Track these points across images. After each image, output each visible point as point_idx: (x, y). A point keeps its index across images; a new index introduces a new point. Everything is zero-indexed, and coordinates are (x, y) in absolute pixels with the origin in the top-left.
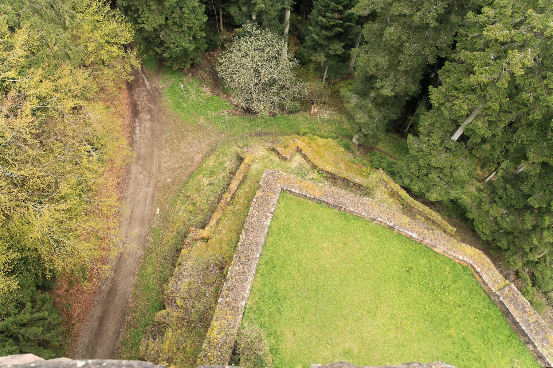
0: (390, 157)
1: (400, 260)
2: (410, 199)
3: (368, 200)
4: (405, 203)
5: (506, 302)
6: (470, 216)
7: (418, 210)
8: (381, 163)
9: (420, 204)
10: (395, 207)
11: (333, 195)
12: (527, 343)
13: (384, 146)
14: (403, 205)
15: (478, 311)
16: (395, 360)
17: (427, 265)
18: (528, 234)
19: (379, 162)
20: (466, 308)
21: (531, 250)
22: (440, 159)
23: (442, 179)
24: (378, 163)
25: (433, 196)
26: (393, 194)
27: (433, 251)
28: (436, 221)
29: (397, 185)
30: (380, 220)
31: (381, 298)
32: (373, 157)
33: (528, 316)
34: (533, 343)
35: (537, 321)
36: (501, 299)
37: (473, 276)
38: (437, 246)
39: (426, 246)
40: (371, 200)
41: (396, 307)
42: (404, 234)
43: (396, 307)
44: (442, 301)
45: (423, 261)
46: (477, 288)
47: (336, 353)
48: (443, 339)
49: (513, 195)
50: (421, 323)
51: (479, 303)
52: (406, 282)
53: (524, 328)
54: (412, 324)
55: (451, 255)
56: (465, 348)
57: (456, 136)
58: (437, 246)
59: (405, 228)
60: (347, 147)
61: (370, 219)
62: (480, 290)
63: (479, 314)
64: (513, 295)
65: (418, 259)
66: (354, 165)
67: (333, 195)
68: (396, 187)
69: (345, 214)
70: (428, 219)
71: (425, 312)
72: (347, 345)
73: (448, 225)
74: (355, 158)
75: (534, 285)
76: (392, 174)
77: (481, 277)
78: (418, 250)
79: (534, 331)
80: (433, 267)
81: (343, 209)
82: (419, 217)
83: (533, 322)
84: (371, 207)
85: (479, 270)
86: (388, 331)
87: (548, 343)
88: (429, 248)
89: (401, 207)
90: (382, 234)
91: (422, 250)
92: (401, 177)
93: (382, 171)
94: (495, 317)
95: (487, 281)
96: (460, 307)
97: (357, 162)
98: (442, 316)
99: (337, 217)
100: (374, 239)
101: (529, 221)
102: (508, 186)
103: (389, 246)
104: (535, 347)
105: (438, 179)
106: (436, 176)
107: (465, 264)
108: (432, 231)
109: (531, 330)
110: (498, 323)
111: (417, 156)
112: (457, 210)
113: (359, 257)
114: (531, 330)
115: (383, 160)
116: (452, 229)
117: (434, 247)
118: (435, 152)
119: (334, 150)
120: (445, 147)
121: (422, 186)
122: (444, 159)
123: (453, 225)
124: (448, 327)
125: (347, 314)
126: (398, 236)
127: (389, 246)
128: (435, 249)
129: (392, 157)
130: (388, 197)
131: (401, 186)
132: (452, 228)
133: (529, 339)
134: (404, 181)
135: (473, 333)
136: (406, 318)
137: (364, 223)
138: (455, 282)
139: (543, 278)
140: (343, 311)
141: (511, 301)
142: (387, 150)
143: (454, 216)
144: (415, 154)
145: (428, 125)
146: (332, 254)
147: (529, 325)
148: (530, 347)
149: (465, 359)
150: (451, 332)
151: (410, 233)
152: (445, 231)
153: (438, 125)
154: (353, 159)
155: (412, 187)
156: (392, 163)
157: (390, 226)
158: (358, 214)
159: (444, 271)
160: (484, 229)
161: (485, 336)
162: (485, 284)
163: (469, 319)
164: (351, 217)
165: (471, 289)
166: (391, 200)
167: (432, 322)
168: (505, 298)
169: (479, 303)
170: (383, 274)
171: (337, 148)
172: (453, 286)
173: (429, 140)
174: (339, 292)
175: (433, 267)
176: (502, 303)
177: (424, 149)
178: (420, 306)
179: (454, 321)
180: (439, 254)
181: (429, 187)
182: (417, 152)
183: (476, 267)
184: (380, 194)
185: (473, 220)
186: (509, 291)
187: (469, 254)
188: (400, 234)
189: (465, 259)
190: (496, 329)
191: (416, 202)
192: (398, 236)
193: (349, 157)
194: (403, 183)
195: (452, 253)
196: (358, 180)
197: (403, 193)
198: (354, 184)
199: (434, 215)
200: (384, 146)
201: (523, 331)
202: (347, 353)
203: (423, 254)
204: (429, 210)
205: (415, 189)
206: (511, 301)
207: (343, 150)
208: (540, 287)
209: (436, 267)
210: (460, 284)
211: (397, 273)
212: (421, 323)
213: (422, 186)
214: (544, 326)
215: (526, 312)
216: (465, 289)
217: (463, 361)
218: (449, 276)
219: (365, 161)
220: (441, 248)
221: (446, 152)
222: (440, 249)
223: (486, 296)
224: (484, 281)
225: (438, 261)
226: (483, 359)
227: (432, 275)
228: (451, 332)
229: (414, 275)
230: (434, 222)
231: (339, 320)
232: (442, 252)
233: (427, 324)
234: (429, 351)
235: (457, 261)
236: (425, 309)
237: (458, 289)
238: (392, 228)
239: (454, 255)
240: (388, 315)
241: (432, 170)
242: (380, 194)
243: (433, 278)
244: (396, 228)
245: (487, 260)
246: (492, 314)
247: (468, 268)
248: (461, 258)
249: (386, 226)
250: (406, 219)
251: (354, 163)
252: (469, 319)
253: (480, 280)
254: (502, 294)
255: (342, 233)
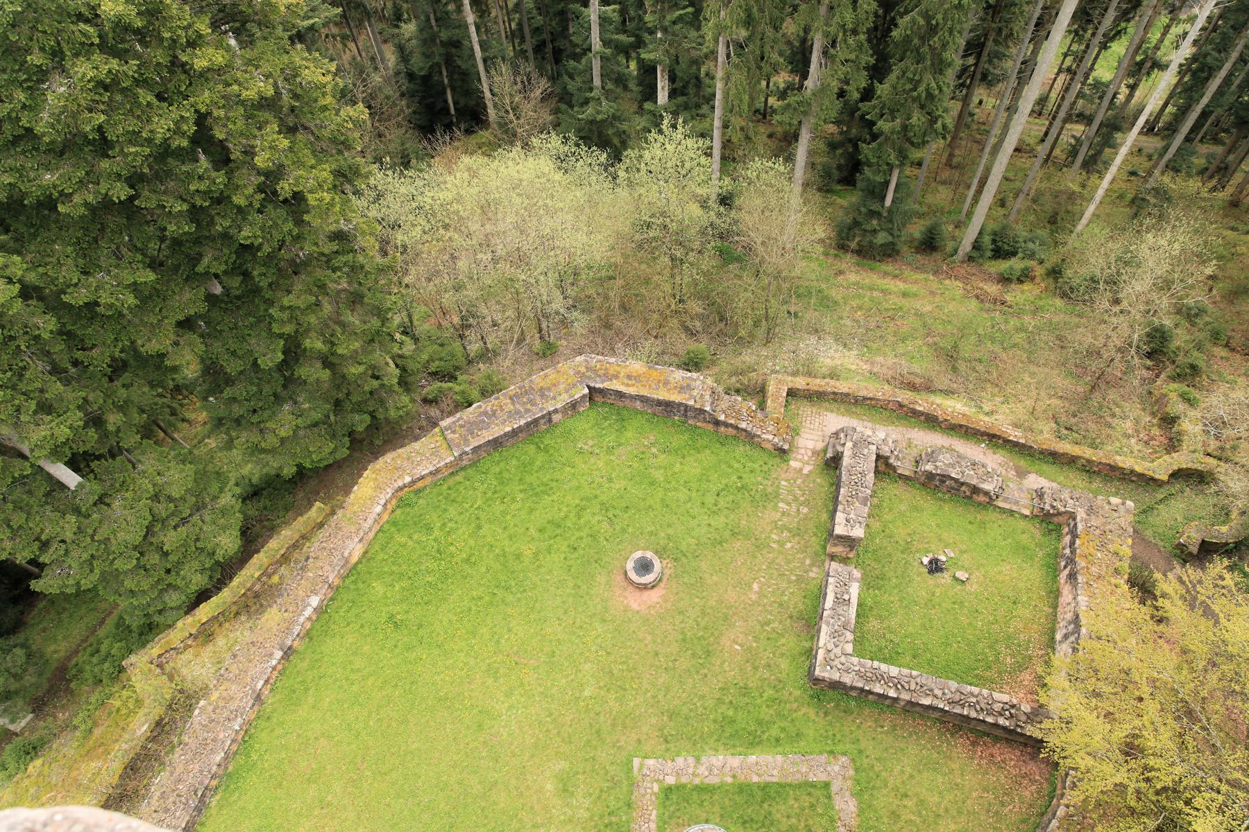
0: (102, 622)
1: (369, 640)
2: (225, 597)
3: (203, 709)
4: (234, 608)
5: (475, 443)
6: (289, 471)
7: (259, 579)
8: (108, 655)
9: (243, 572)
10: (240, 633)
11: (167, 810)
12: (550, 421)
13: (64, 638)
14: (237, 613)
15: (489, 494)
16: (580, 675)
17: (388, 580)
18: (340, 380)
19: (105, 660)
20: (482, 515)
21: (377, 378)
22: (124, 521)
23: (184, 521)
24: (107, 665)
25: (228, 543)
26: (205, 634)
27: (357, 563)
28: (291, 542)
29: (180, 624)
30: (261, 683)
31: (450, 696)
32: (87, 675)
33: (502, 410)
34: (550, 413)
35: (511, 398)
36: (467, 449)
37: (419, 491)
38: (346, 554)
39: (344, 578)
40: (202, 703)
41: (472, 662)
42: (308, 625)
43: (472, 662)
44: (467, 561)
45: (379, 588)
46: (445, 487)
47: (565, 813)
48: (542, 570)
49: (249, 388)
50: (509, 611)
51: (475, 489)
52: (421, 632)
53: (522, 422)
54: (510, 630)
55: (370, 529)
56: (558, 531)
57: (70, 478)
58: (346, 554)
59: (292, 622)
60: (32, 750)
61: (256, 708)
62: (451, 482)
63: (495, 492)
64: (461, 426)
65: (373, 598)
66: (97, 732)
67: (167, 810)
68: (187, 624)
69: (230, 776)
70: (285, 559)
71: (487, 599)
72: (549, 787)
73: (306, 516)
74: (76, 728)
75: (453, 378)
76: (149, 630)
77: (423, 478)
78: (351, 597)
79: (529, 406)
80: (394, 568)
81: (214, 783)
82: (275, 579)
83: (513, 404)
84: (221, 704)
85: (408, 479)
86: (522, 684)
87: (549, 389)
88: (351, 571)
89: (243, 618)
90: (299, 679)
91: (352, 587)
92: (160, 612)
93: (133, 658)
94: (502, 464)
95: (432, 468)
96: (479, 527)
97: (90, 723)
98: (497, 566)
99: (234, 798)
100: (311, 700)
101: (312, 372)
102: (228, 392)
103: (334, 664)
104: (556, 411)
105: (182, 530)
106: (173, 533)
107: (394, 502)
108: (311, 560)
109: (527, 411)
110: (514, 462)
111: (103, 573)
112: (275, 489)
113: (349, 744)
114: (527, 411)
115: (104, 648)
116: (316, 511)
117: (347, 562)
118: (100, 531)
119: (32, 791)
120: (95, 504)
121: (196, 565)
122: (126, 512)
123: (310, 505)
124: (518, 557)
125: (480, 783)
126: (311, 639)
127: (334, 664)
128: (354, 559)
129: (104, 619)
130: (210, 647)
131: (187, 613)
132: (314, 509)
133: (543, 417)
134: (173, 604)
135: (531, 511)
136: (498, 642)
137: (262, 723)
138: (429, 529)
139: (441, 359)
140: (474, 791)
141: (472, 433)
142: (77, 630)
143: (289, 498)
144: (95, 577)
145: (12, 539)
146: (333, 818)
147: (518, 412)
148: (556, 418)
149: (578, 534)
150: (528, 551)
151: (308, 612)
152: (321, 525)
153: (18, 519)
154: (78, 734)
155: (194, 588)
156: (118, 626)
157: (282, 658)
158: (233, 741)
159: (404, 546)
160: (321, 450)
161: (538, 490)
162: (438, 471)
163: (504, 513)
164: (241, 759)
165: (446, 498)
166: (221, 642)
167: (507, 588)
168: (466, 442)
169: (475, 489)
170: (396, 685)
171: (27, 782)
172: (436, 533)
173: (63, 541)
174: (430, 802)
175: (394, 568)
176: (475, 450)
177: (85, 556)
178: (474, 608)
179: (506, 542)
180: (366, 552)
181: (202, 550)
182: (92, 571)
183: (400, 483)
184: (196, 667)
185: (299, 466)
186: (454, 432)
187: (373, 489)
188: (307, 635)
189: (382, 502)
190: (525, 467)
191: (236, 581)
192: (311, 639)
193: (67, 747)
194: (178, 608)
195: (366, 526)
196: (141, 727)
197: (205, 611)
198: (153, 739)
199: (275, 545)
200: (64, 638)
201: (528, 425)
202: (565, 790)
203: (361, 586)
204: (261, 554)
205: (199, 581)
206: (472, 433)
207: (38, 762)
208: (457, 368)
209: (393, 563)
210: (435, 519)
211: (397, 651)
212: (509, 611)
213: (196, 565)
214: (520, 388)
215: (494, 412)
216: (445, 510)
217: (581, 538)
218: (415, 537)
219: (93, 700)
220: (351, 546)
221: (108, 505)
222: (355, 550)
223: (462, 473)
224: (431, 473)
225: (381, 556)
226: (577, 501)
227: (410, 574)
228: (528, 551)
229: (407, 612)
230: (295, 546)
231: (495, 803)
232: (360, 545)
233: (510, 598)
234: (564, 602)
235: (385, 517)
236: (481, 598)
237: (444, 525)
238: (288, 652)
239: (370, 521)
240: (490, 681)
241: (153, 540)
242: (196, 667)
243: (416, 573)
244: (289, 643)
245: (389, 457)
246: (497, 470)
247: (405, 498)
248: (379, 509)
249: (280, 667)
250: (272, 617)
251: (90, 731)
252: (504, 513)
253: (428, 480)
254: (458, 445)
255: (280, 785)
